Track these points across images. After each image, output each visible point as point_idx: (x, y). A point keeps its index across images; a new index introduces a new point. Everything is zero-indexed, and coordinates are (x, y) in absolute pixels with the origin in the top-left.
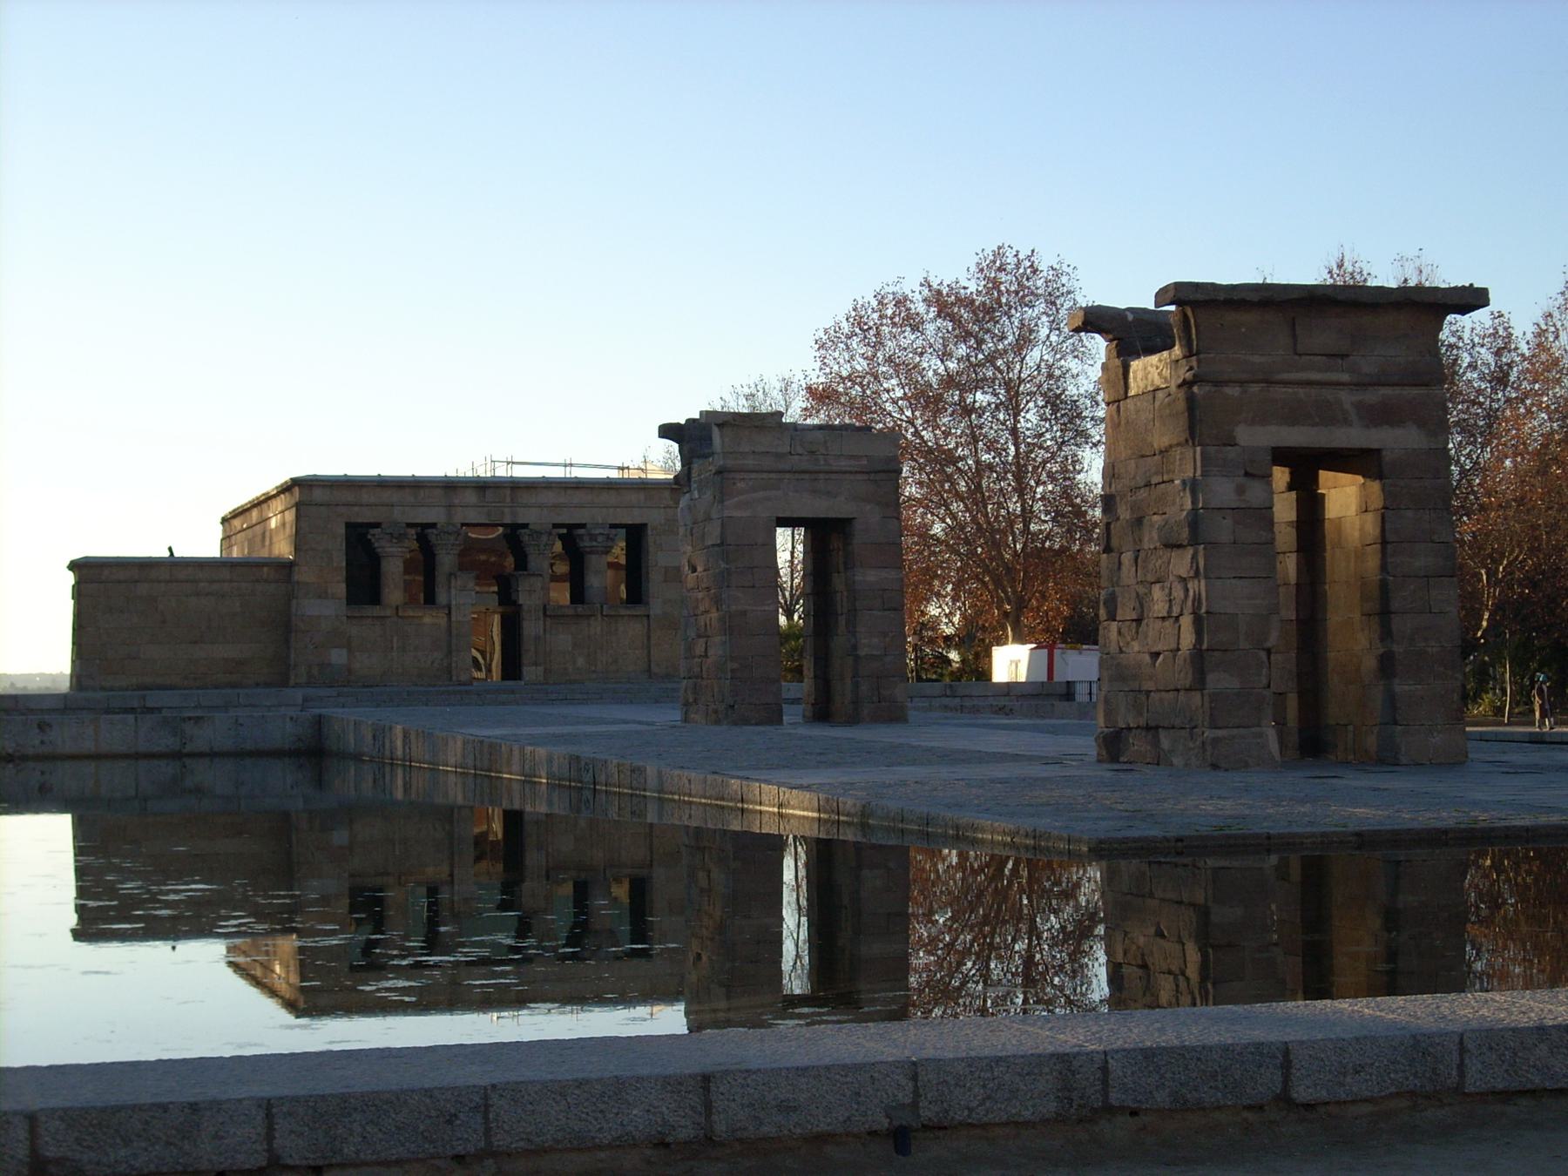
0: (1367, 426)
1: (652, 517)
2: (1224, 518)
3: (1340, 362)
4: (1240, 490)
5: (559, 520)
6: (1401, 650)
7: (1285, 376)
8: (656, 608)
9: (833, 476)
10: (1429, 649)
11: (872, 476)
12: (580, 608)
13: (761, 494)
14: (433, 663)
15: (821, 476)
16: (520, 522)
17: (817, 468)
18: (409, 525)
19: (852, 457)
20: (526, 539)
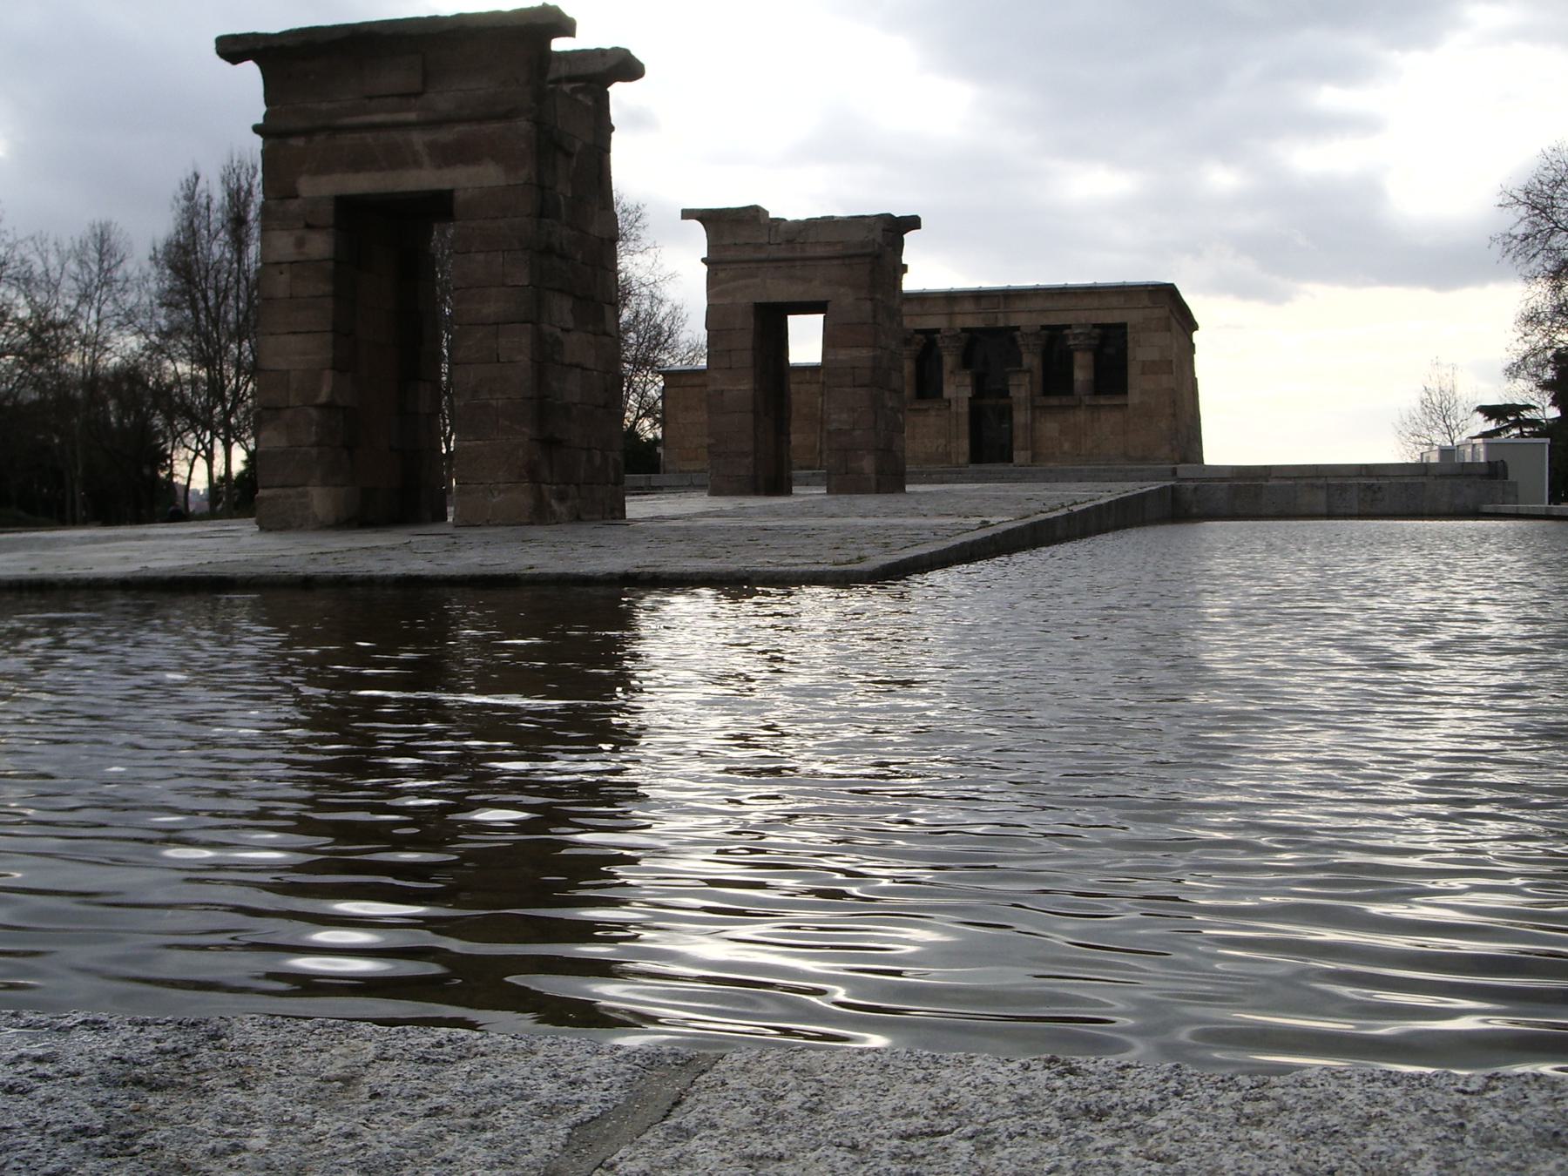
0: (439, 167)
1: (1132, 317)
2: (281, 273)
3: (413, 101)
4: (300, 243)
5: (1045, 322)
6: (462, 404)
7: (347, 121)
8: (1134, 397)
9: (808, 263)
10: (494, 402)
11: (847, 261)
12: (1065, 400)
13: (741, 282)
14: (938, 447)
15: (798, 263)
16: (1012, 324)
17: (790, 255)
18: (918, 331)
19: (828, 244)
20: (1020, 341)
